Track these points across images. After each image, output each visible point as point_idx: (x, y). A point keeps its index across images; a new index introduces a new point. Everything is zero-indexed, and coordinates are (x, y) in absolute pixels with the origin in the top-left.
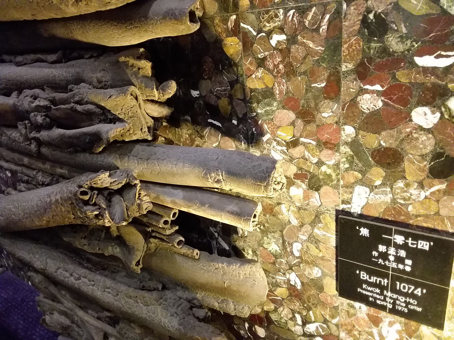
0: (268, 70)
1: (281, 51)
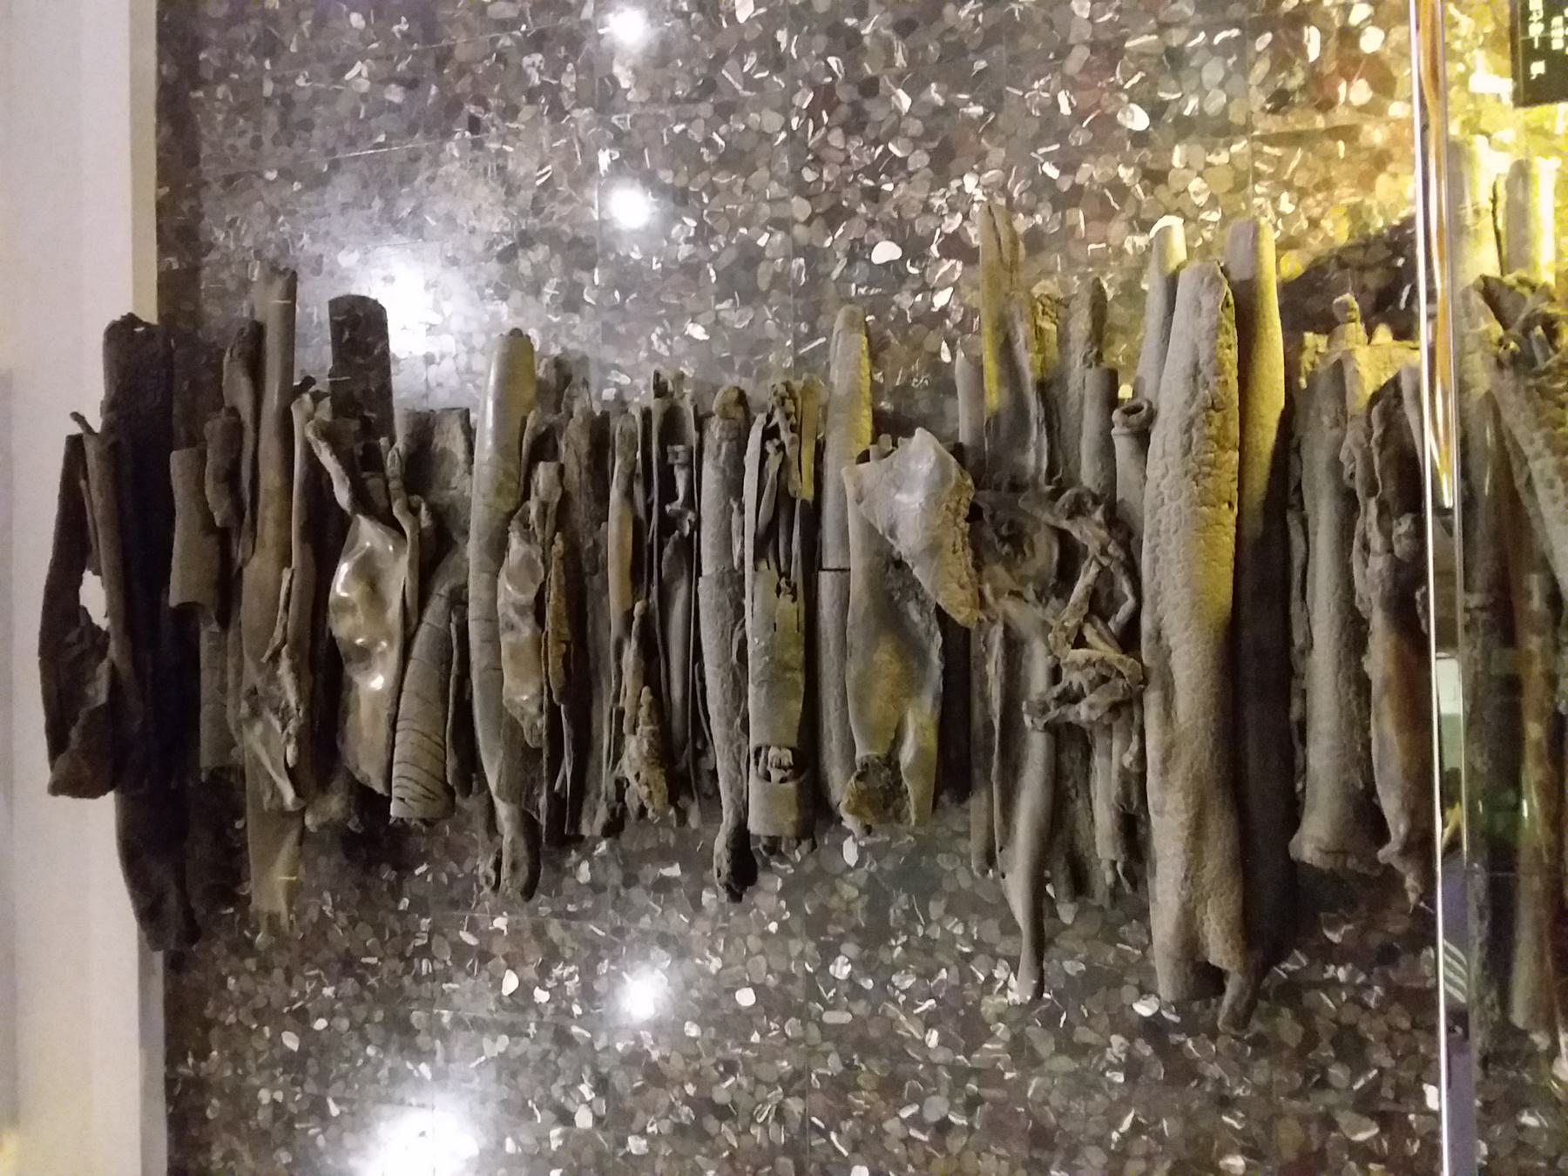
0: (1323, 213)
1: (1300, 199)
